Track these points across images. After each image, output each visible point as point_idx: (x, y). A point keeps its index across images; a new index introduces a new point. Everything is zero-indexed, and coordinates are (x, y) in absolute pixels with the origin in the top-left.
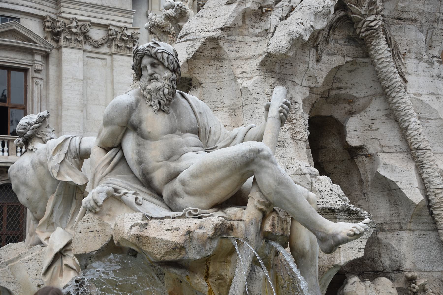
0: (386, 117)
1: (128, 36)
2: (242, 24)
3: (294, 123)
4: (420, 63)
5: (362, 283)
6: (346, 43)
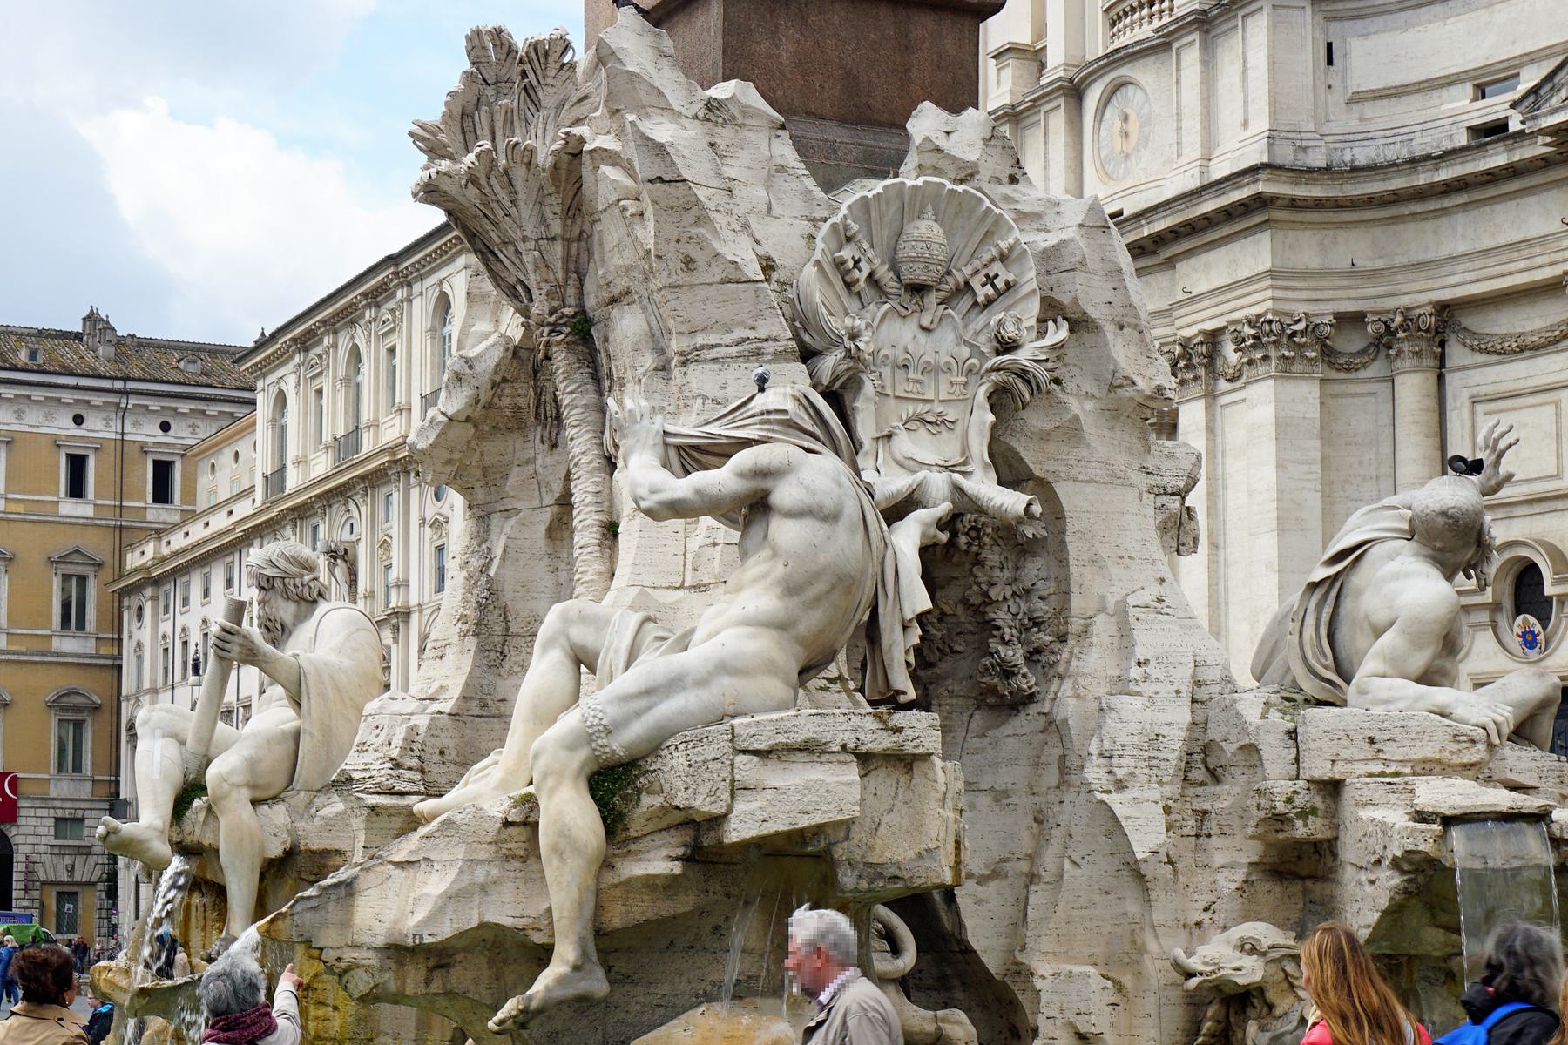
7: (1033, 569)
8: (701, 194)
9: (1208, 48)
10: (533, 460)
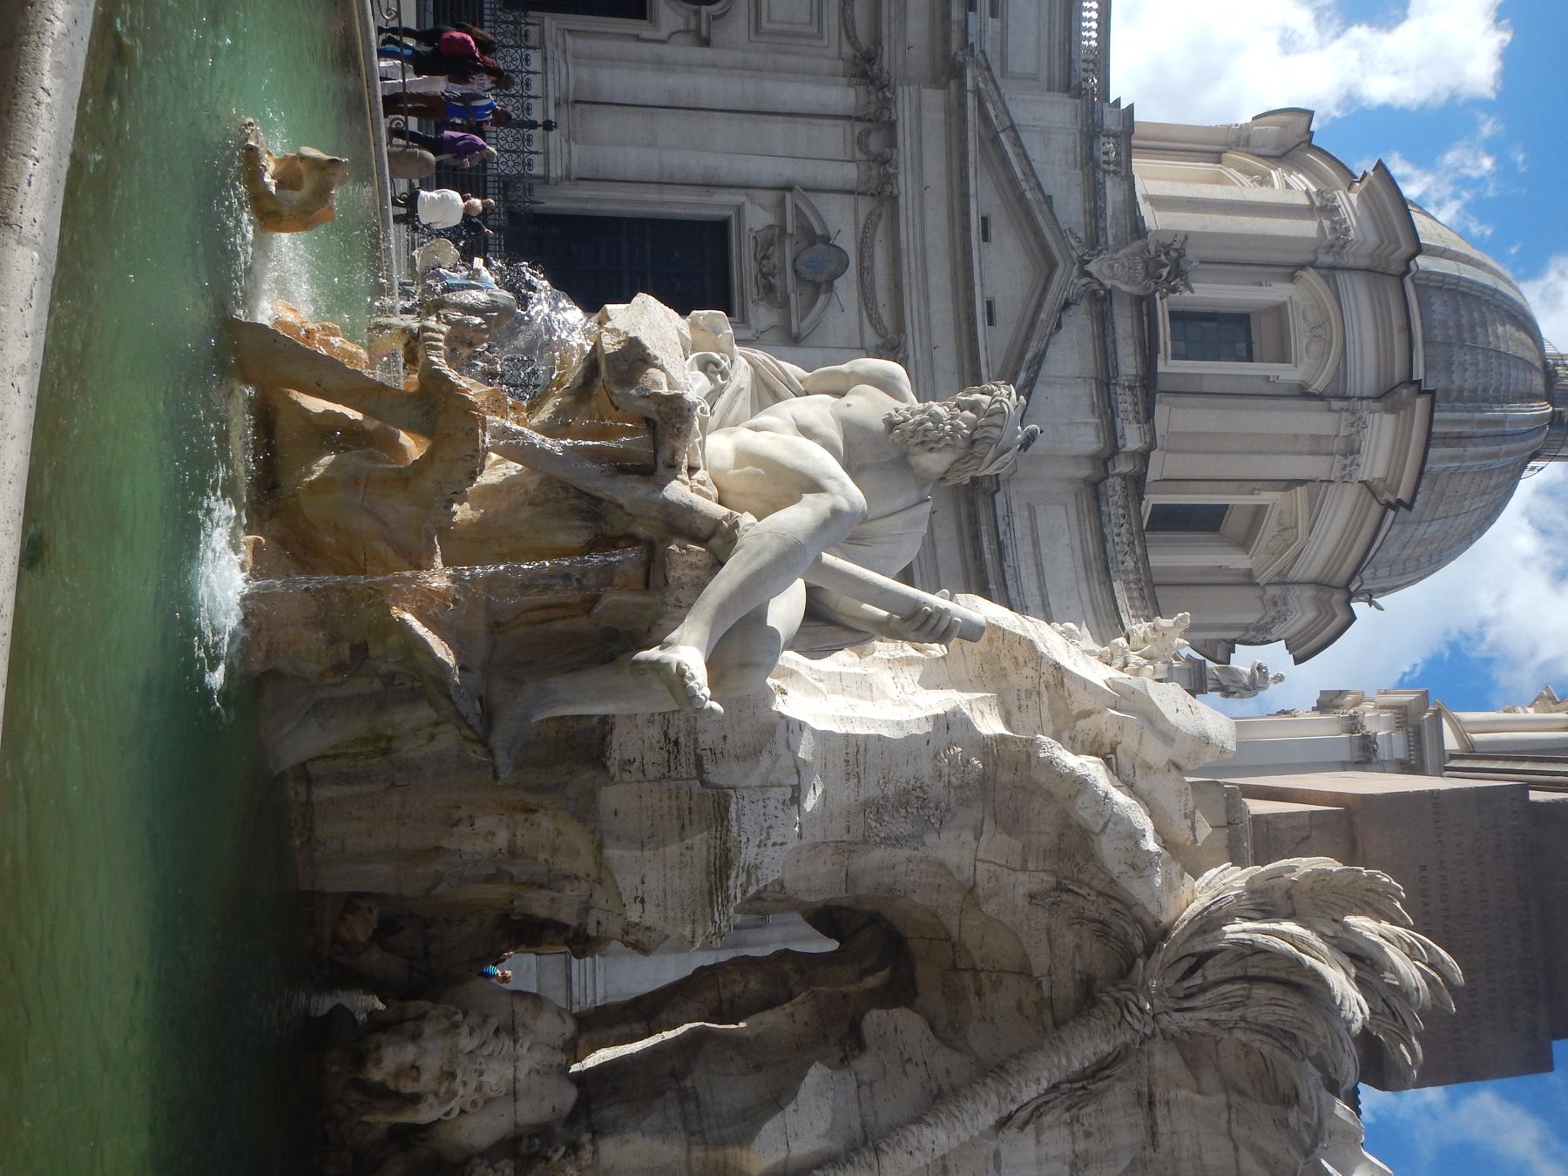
0: (936, 1092)
2: (1074, 713)
3: (898, 812)
4: (1067, 1168)
5: (560, 1042)
6: (1078, 977)
10: (1024, 869)
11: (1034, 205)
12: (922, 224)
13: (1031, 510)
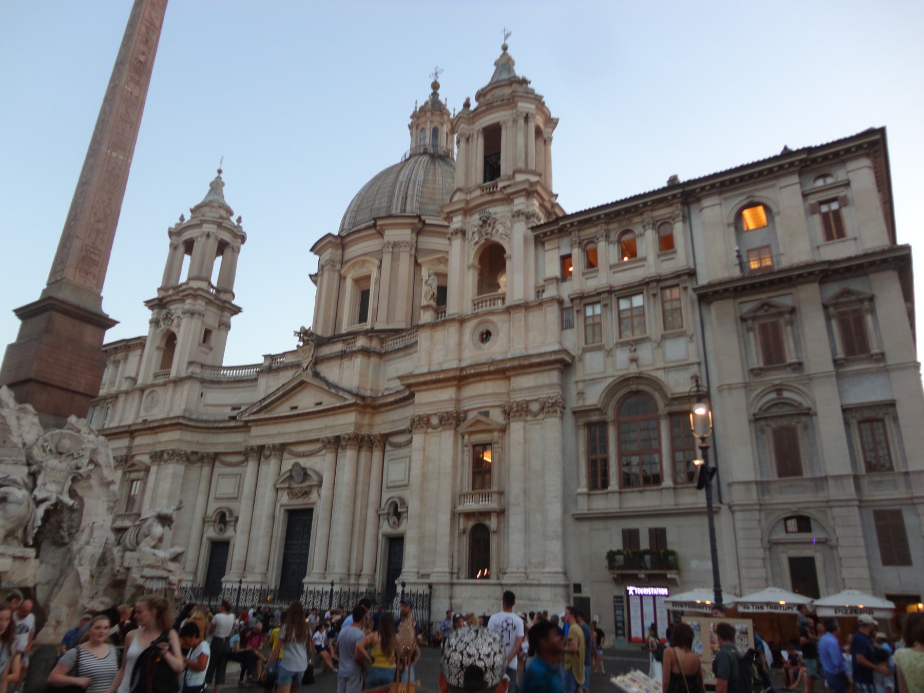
1: (553, 404)
7: (75, 515)
8: (11, 428)
9: (175, 388)
11: (284, 391)
12: (290, 433)
13: (389, 380)
